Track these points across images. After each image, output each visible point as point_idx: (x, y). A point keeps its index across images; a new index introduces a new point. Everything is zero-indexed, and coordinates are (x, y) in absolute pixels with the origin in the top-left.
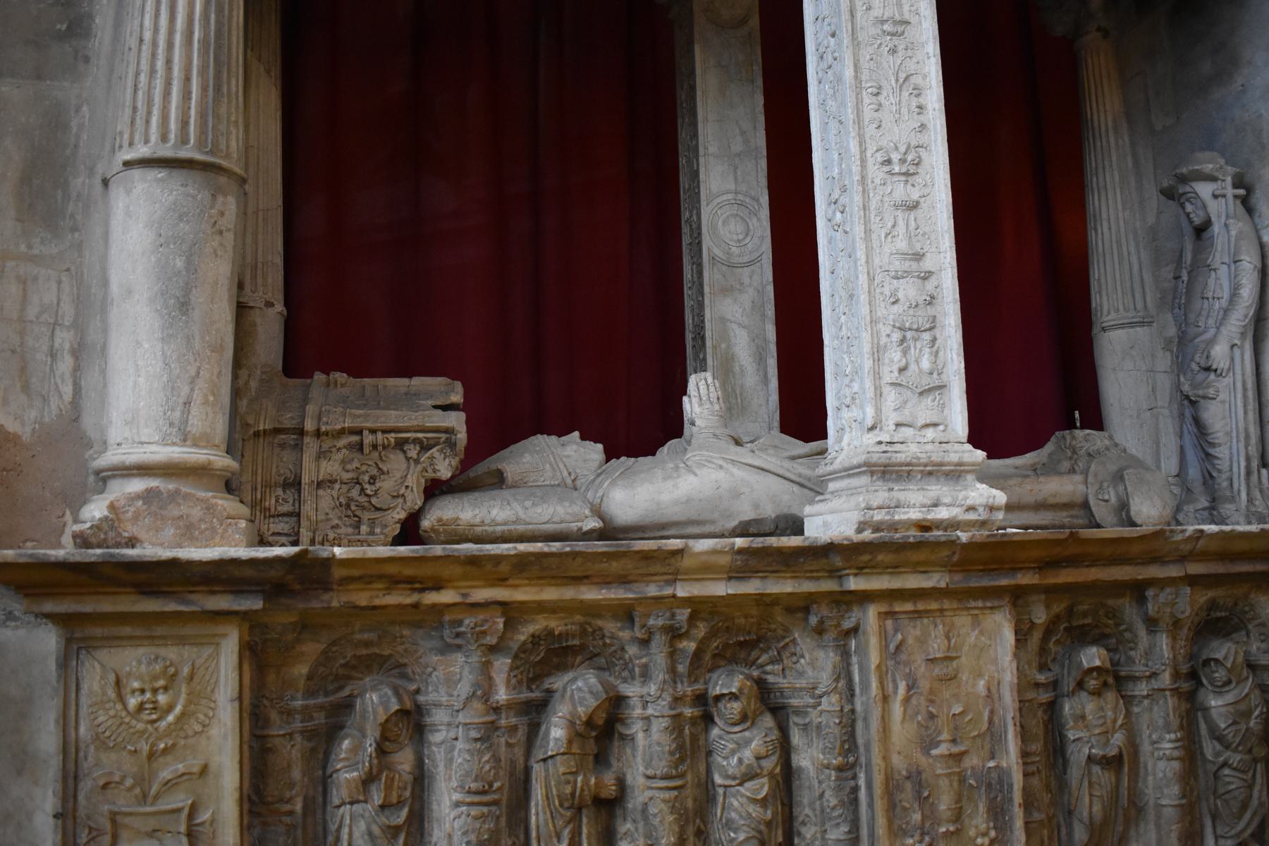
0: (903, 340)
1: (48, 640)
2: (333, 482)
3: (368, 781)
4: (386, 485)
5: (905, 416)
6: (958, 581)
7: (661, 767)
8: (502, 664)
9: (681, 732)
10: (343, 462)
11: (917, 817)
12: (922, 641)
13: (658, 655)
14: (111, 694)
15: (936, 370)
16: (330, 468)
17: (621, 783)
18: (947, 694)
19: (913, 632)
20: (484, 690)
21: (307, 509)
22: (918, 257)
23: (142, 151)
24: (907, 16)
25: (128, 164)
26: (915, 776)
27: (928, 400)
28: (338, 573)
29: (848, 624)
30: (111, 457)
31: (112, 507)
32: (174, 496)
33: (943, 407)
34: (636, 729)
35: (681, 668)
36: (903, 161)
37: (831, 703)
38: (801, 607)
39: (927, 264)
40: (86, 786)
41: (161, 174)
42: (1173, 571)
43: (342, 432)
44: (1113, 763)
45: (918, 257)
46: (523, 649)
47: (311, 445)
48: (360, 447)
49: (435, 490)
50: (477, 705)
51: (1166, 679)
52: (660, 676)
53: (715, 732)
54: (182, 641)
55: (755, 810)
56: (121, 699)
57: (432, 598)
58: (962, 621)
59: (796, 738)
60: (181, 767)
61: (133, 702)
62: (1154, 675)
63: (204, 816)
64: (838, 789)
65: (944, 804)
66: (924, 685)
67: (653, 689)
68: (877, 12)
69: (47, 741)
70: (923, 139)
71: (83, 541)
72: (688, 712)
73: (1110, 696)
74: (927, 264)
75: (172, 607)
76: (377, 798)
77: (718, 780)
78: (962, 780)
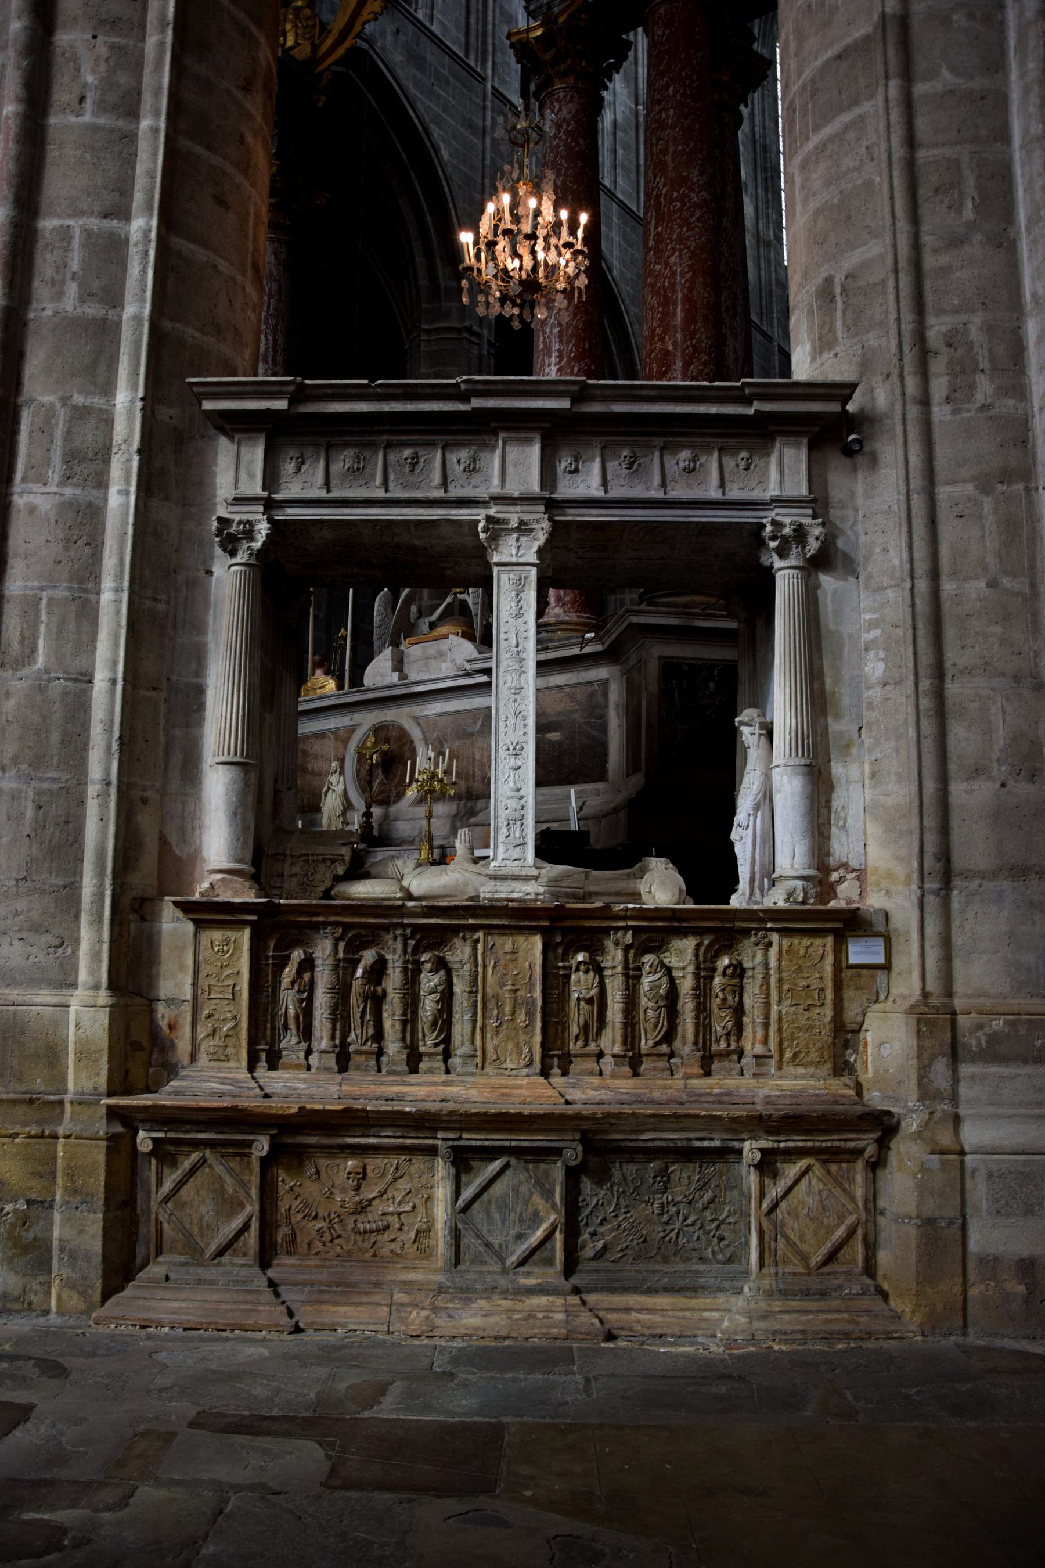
0: (508, 824)
1: (190, 927)
2: (296, 875)
3: (293, 983)
4: (318, 876)
5: (507, 856)
6: (513, 923)
7: (398, 985)
8: (342, 945)
9: (407, 974)
10: (302, 867)
11: (495, 1012)
12: (503, 945)
13: (399, 945)
14: (209, 945)
15: (523, 836)
16: (296, 869)
17: (384, 992)
18: (511, 966)
19: (499, 940)
20: (336, 951)
21: (286, 885)
22: (519, 790)
23: (221, 759)
24: (523, 685)
25: (217, 763)
26: (496, 997)
27: (518, 849)
28: (283, 909)
29: (475, 937)
30: (211, 867)
31: (211, 884)
32: (231, 881)
33: (524, 852)
34: (390, 971)
35: (409, 950)
36: (514, 749)
37: (467, 967)
38: (456, 930)
39: (522, 793)
40: (201, 976)
41: (228, 767)
42: (622, 924)
43: (300, 856)
44: (590, 1001)
45: (519, 790)
46: (350, 939)
47: (289, 861)
48: (308, 861)
49: (338, 879)
50: (332, 958)
51: (619, 969)
52: (399, 950)
53: (422, 975)
54: (232, 929)
55: (434, 1005)
56: (212, 947)
57: (315, 919)
58: (521, 939)
59: (455, 981)
60: (230, 972)
61: (216, 949)
62: (614, 967)
63: (237, 988)
64: (468, 1000)
65: (508, 1009)
66: (502, 962)
67: (397, 957)
68: (508, 685)
69: (189, 961)
70: (526, 738)
71: (202, 894)
72: (410, 966)
73: (591, 974)
74: (522, 793)
75: (228, 918)
76: (296, 987)
77: (422, 993)
78: (515, 999)
